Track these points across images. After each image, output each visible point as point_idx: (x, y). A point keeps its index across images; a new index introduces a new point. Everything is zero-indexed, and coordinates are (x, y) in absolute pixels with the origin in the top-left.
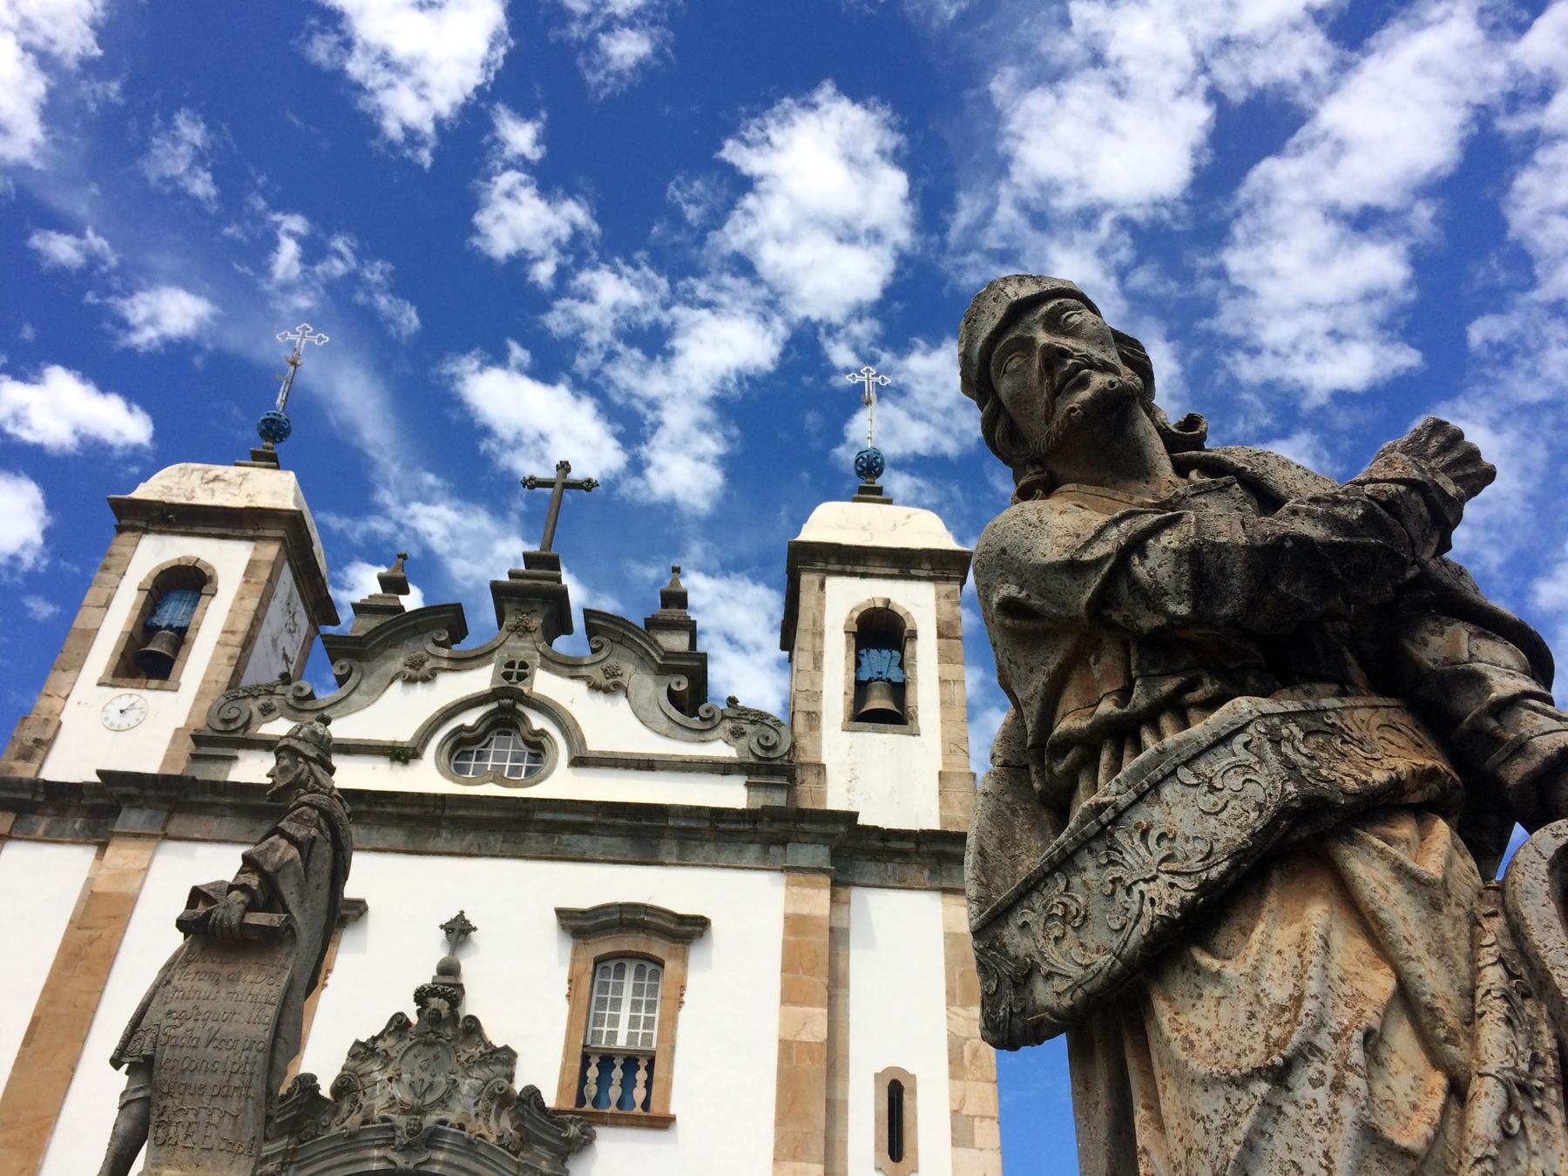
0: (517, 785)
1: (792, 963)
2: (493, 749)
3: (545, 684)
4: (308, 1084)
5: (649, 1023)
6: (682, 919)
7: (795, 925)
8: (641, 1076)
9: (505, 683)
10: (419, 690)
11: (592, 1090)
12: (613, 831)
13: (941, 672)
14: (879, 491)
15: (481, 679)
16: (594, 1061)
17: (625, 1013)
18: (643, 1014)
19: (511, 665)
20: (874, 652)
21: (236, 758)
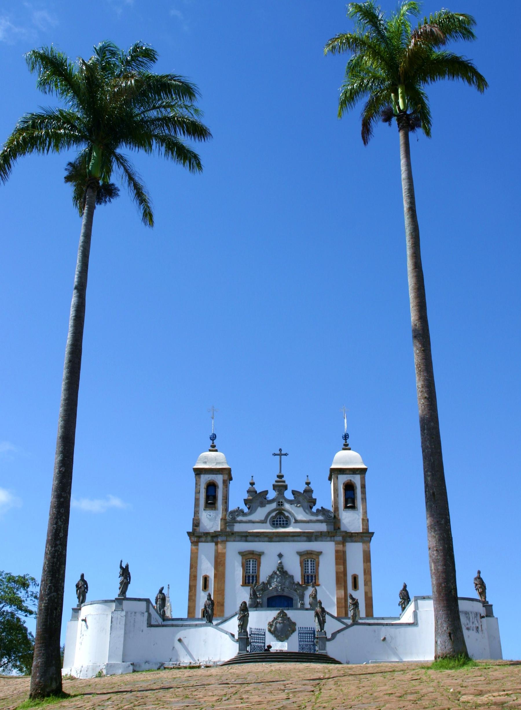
0: (284, 527)
1: (337, 559)
2: (278, 520)
3: (287, 506)
4: (263, 583)
5: (314, 569)
6: (318, 552)
7: (337, 552)
8: (314, 578)
9: (278, 507)
10: (263, 509)
11: (306, 581)
12: (304, 536)
13: (362, 496)
14: (347, 445)
15: (274, 506)
16: (306, 576)
17: (310, 568)
18: (312, 568)
19: (279, 502)
20: (348, 492)
21: (234, 525)
